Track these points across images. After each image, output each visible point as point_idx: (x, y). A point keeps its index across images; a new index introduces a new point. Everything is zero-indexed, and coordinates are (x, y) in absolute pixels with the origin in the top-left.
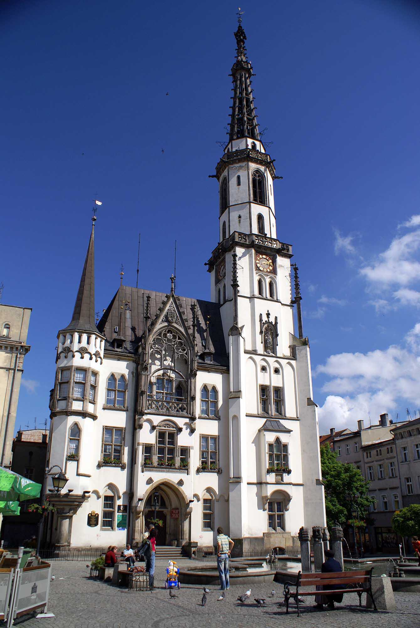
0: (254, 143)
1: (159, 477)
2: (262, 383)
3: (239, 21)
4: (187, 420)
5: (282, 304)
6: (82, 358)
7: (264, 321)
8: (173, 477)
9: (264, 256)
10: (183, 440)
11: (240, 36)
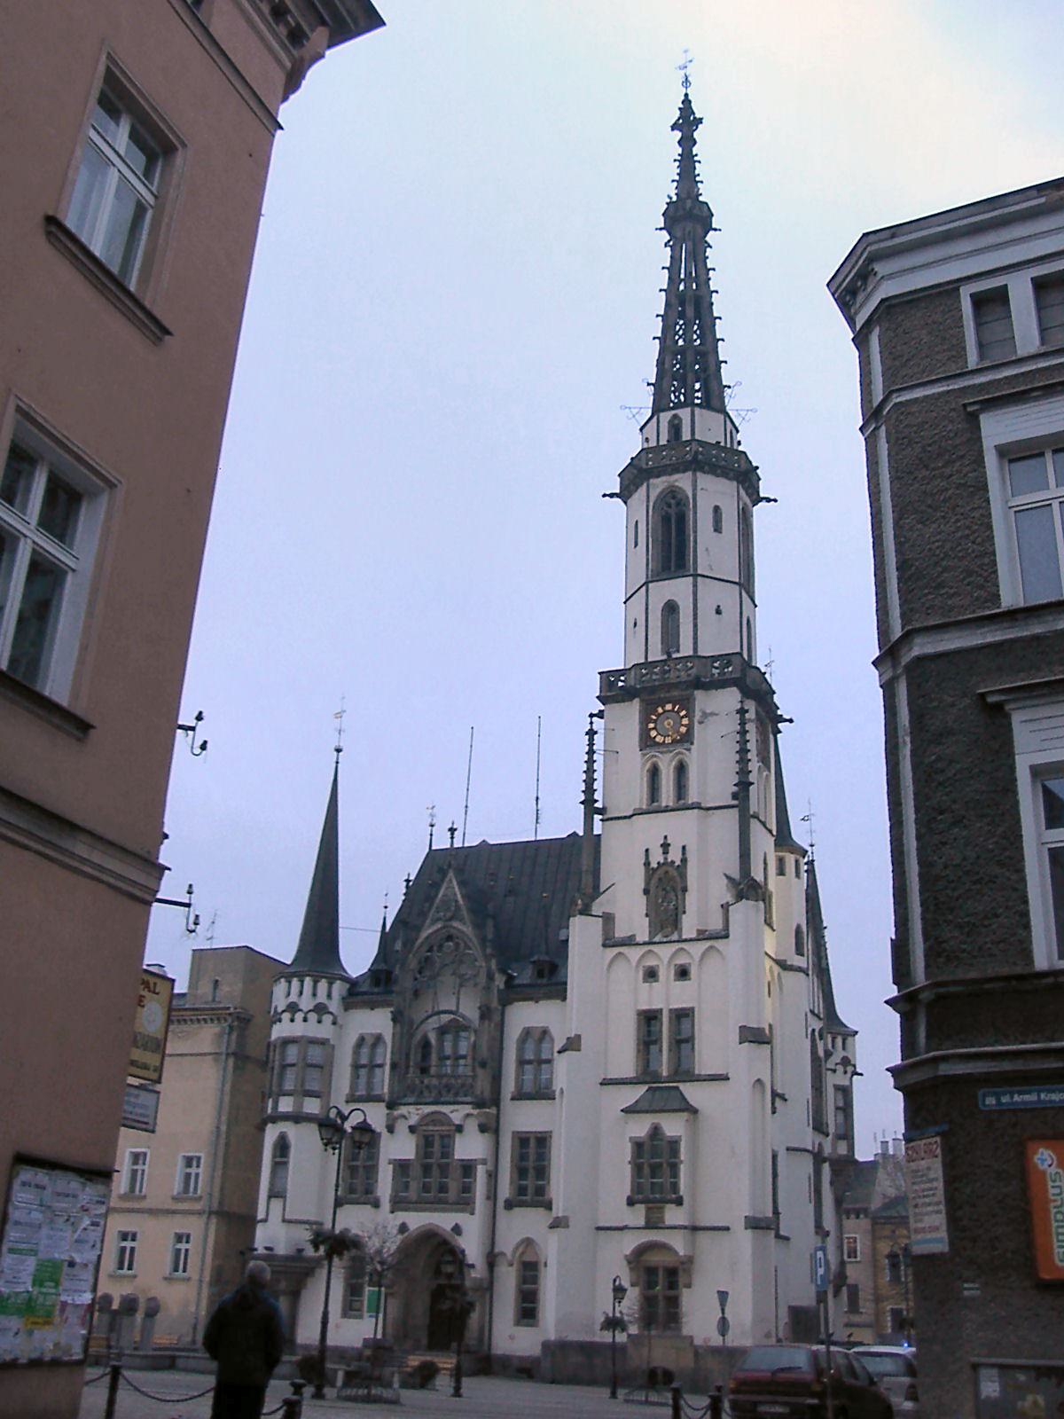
0: (675, 416)
1: (417, 1220)
2: (645, 1007)
3: (686, 83)
4: (468, 1109)
5: (709, 809)
6: (292, 1020)
7: (654, 865)
8: (443, 1221)
9: (669, 707)
10: (471, 1146)
11: (687, 122)
